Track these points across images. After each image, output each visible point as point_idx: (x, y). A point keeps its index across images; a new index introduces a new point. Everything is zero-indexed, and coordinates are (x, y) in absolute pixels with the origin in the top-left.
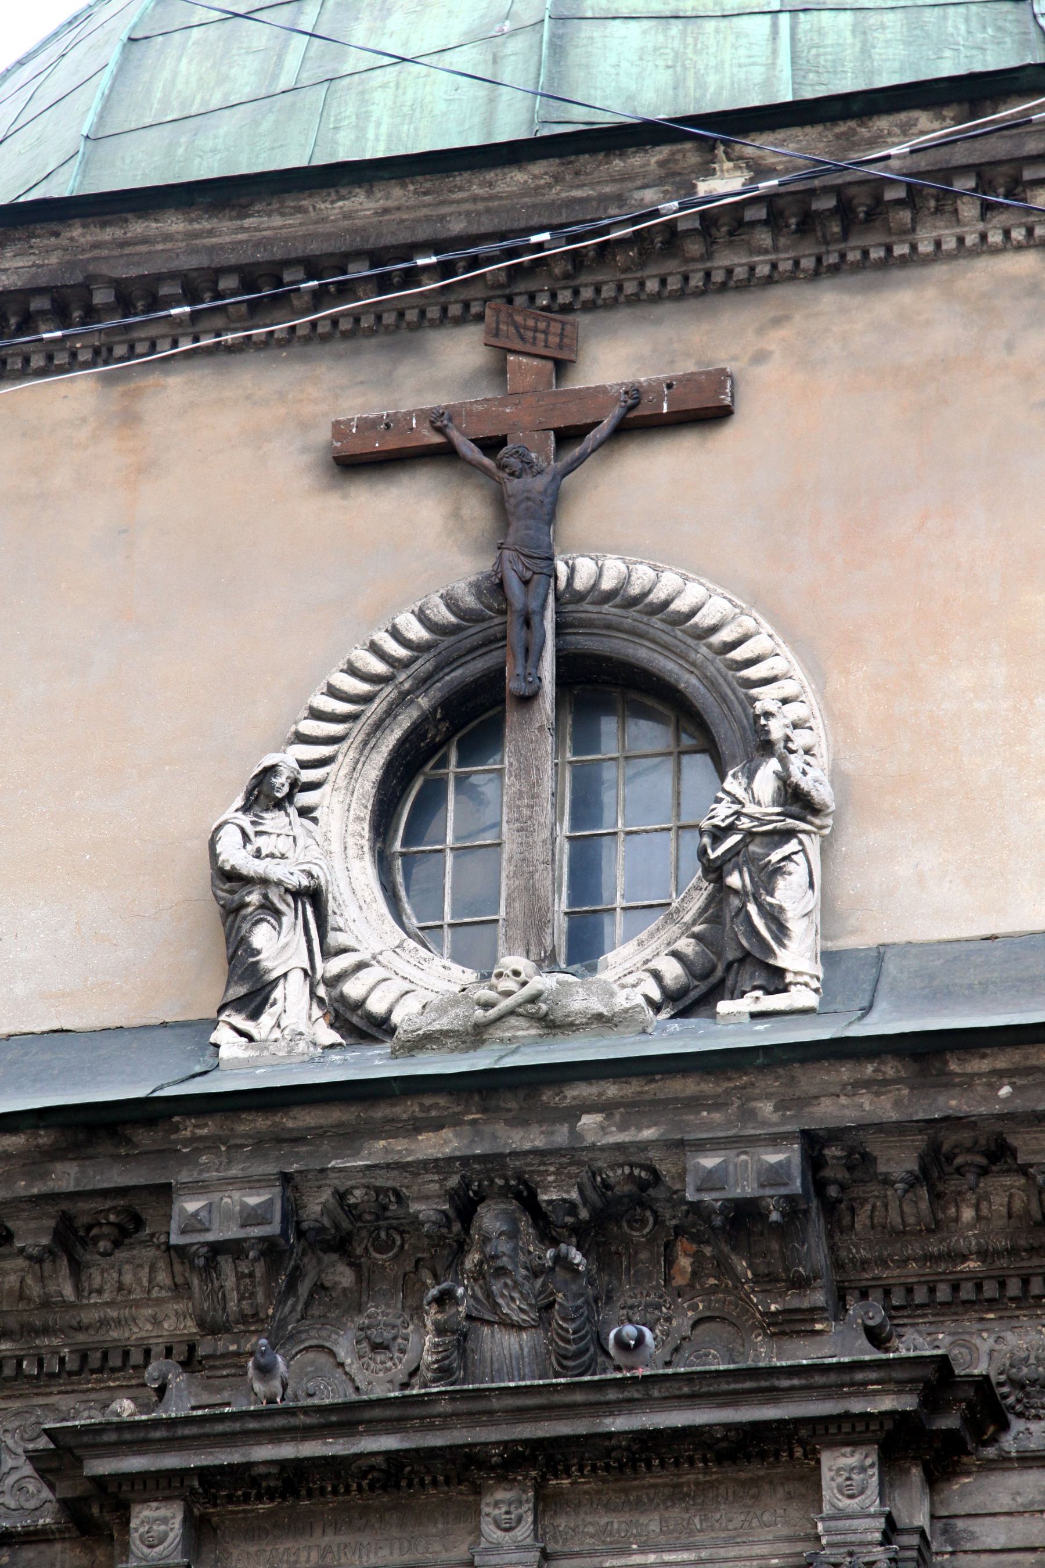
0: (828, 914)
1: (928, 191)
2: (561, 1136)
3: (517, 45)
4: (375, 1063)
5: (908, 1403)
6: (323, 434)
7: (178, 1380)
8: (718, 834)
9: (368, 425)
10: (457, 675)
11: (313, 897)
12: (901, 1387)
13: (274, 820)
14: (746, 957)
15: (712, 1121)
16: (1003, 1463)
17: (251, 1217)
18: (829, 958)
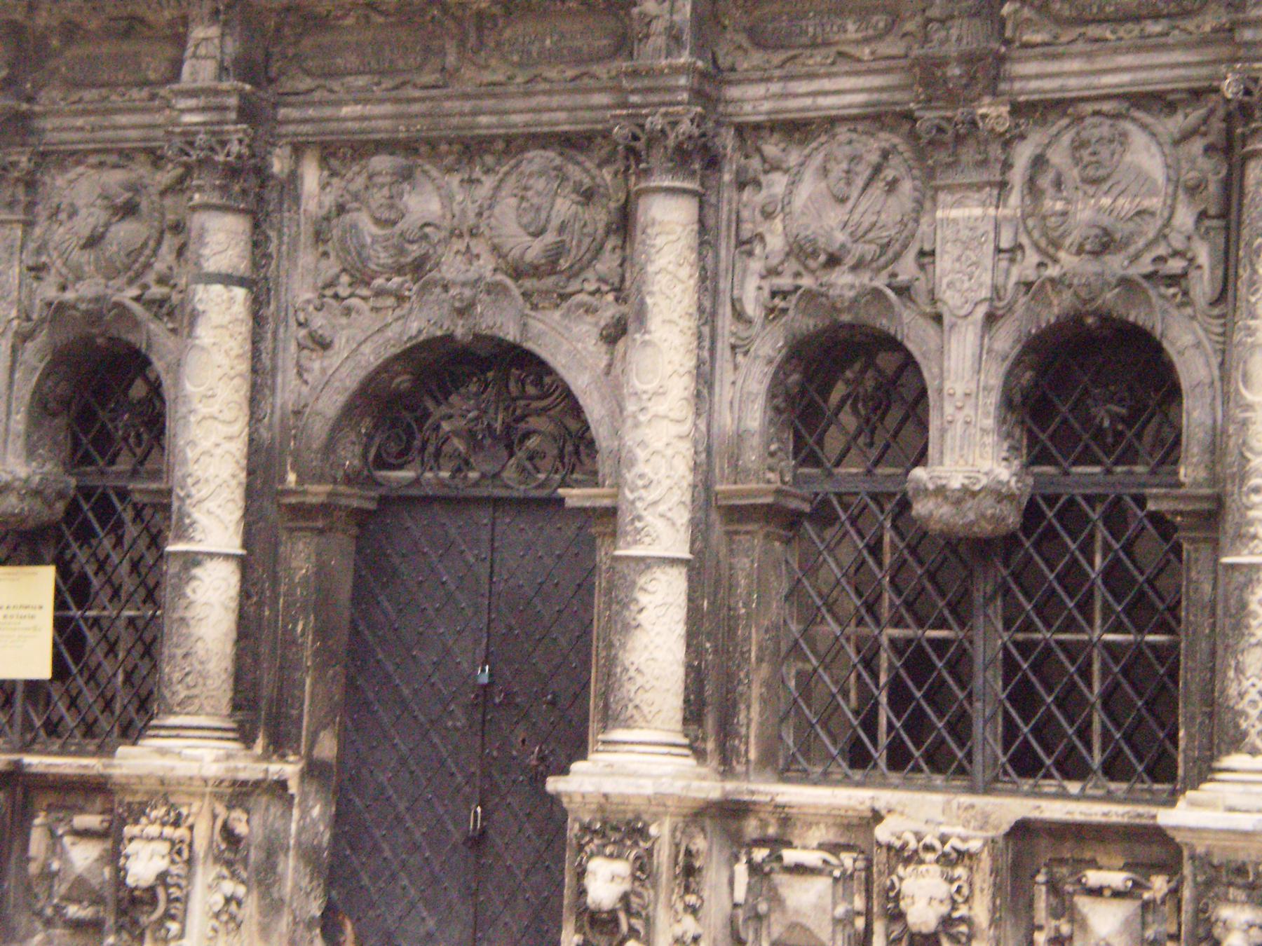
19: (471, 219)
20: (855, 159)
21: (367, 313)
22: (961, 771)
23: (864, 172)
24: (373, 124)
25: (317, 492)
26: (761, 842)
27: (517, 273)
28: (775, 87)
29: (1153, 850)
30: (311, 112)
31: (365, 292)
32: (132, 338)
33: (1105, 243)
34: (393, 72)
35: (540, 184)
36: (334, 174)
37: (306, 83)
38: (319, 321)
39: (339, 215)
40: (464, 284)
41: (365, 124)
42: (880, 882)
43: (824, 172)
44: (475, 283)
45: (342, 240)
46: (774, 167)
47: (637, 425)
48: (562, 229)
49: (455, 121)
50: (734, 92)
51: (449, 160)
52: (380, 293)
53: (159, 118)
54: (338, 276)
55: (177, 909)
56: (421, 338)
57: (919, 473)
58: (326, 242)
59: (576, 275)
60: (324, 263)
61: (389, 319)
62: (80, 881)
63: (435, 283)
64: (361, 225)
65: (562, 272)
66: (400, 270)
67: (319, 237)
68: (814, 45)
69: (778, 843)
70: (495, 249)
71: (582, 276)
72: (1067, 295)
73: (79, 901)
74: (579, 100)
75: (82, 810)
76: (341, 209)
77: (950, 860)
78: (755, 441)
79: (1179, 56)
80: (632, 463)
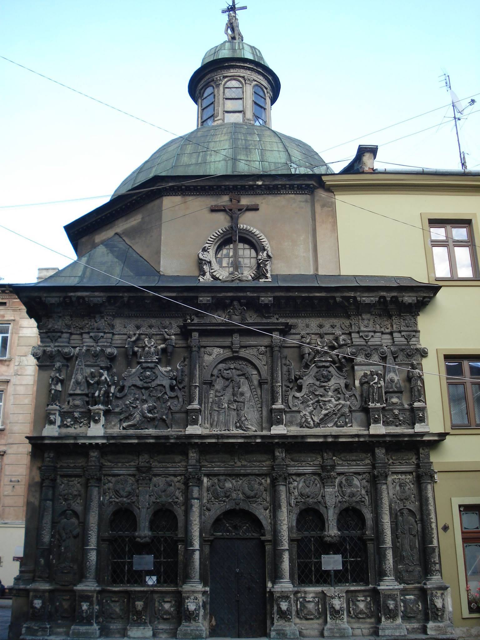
0: (271, 270)
1: (284, 187)
2: (245, 294)
3: (229, 162)
4: (219, 284)
5: (284, 327)
6: (210, 206)
7: (196, 318)
8: (260, 260)
9: (215, 206)
10: (226, 237)
11: (210, 262)
12: (283, 326)
13: (205, 253)
14: (263, 274)
15: (263, 294)
16: (291, 334)
17: (208, 301)
18: (271, 275)
20: (311, 480)
22: (328, 584)
23: (312, 483)
25: (211, 538)
26: (301, 597)
27: (248, 497)
28: (296, 468)
29: (375, 593)
32: (171, 508)
33: (352, 495)
34: (224, 462)
35: (253, 482)
36: (210, 479)
37: (206, 464)
38: (209, 506)
42: (328, 602)
43: (305, 482)
44: (240, 499)
45: (213, 491)
46: (295, 481)
47: (281, 525)
50: (289, 468)
52: (221, 501)
53: (178, 469)
55: (198, 615)
57: (326, 533)
62: (167, 611)
66: (226, 497)
67: (208, 490)
68: (303, 461)
69: (304, 598)
70: (243, 493)
72: (347, 504)
73: (166, 615)
75: (165, 597)
76: (213, 486)
77: (339, 598)
78: (295, 528)
79: (362, 467)
80: (280, 532)
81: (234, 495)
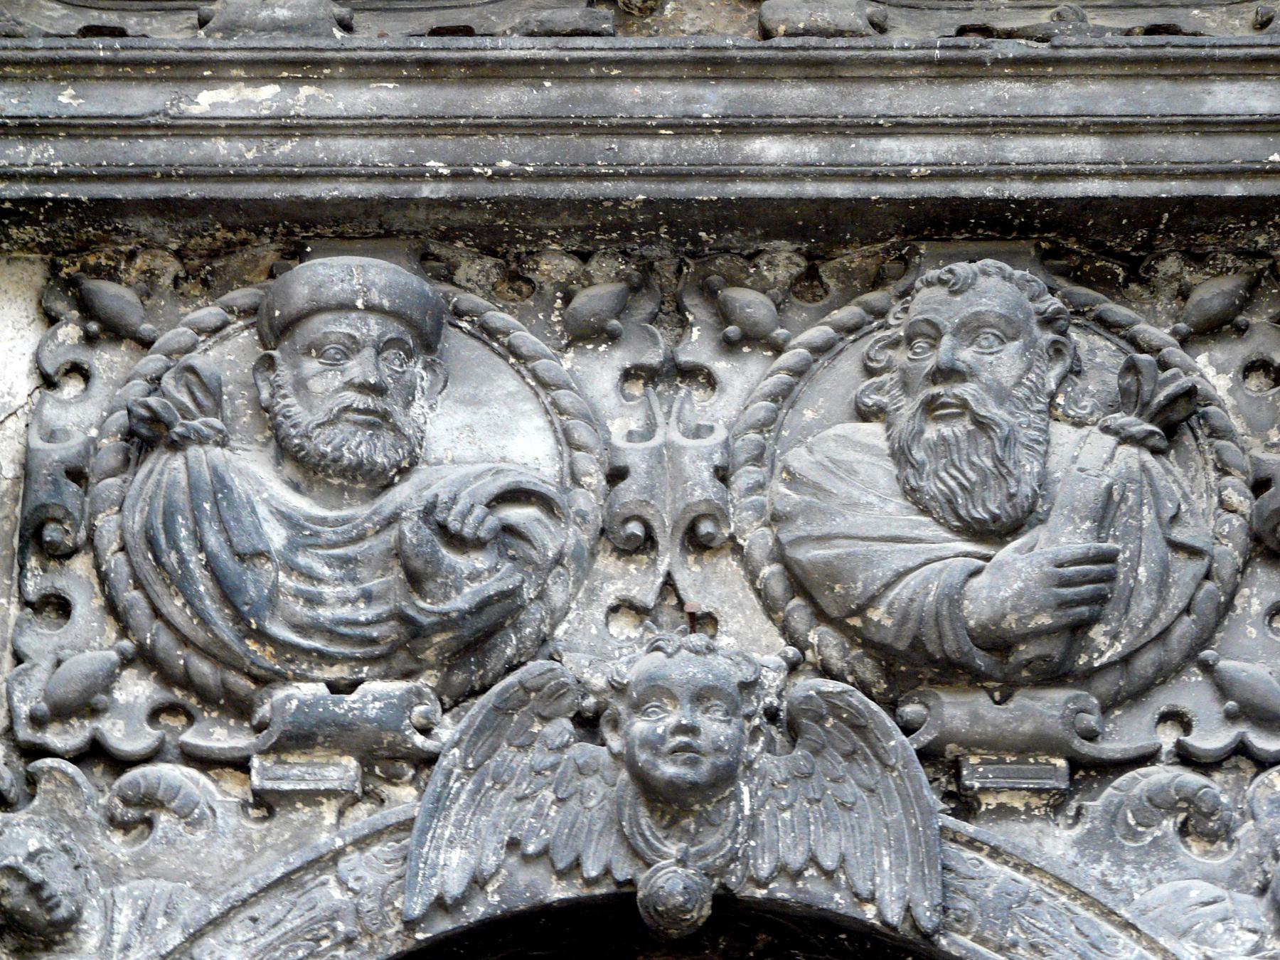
19: (702, 489)
21: (229, 819)
24: (319, 149)
27: (912, 664)
30: (68, 100)
31: (220, 737)
35: (1006, 363)
39: (128, 464)
40: (701, 696)
41: (286, 148)
48: (1105, 512)
49: (649, 150)
51: (596, 296)
54: (108, 681)
56: (477, 911)
58: (59, 555)
59: (1137, 695)
60: (41, 639)
61: (325, 839)
63: (548, 698)
64: (239, 485)
65: (1087, 677)
66: (402, 647)
71: (1163, 700)
74: (1155, 97)
81: (596, 644)
